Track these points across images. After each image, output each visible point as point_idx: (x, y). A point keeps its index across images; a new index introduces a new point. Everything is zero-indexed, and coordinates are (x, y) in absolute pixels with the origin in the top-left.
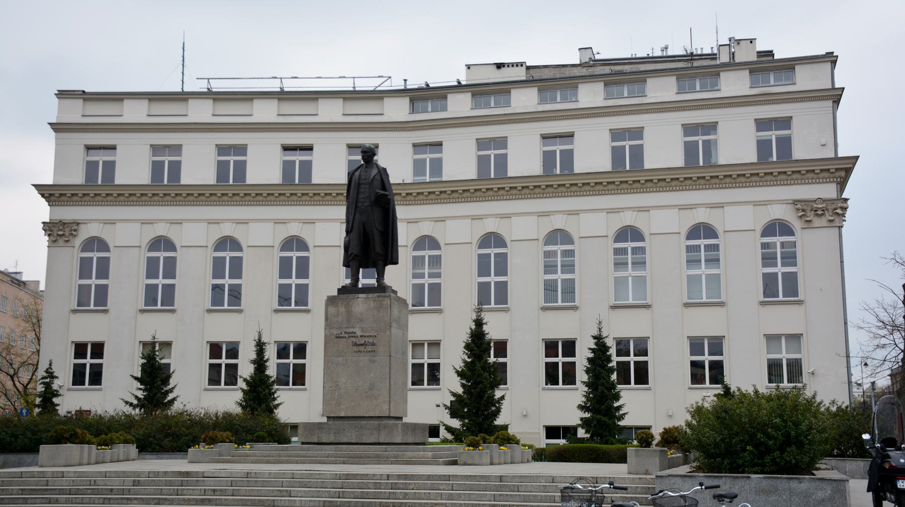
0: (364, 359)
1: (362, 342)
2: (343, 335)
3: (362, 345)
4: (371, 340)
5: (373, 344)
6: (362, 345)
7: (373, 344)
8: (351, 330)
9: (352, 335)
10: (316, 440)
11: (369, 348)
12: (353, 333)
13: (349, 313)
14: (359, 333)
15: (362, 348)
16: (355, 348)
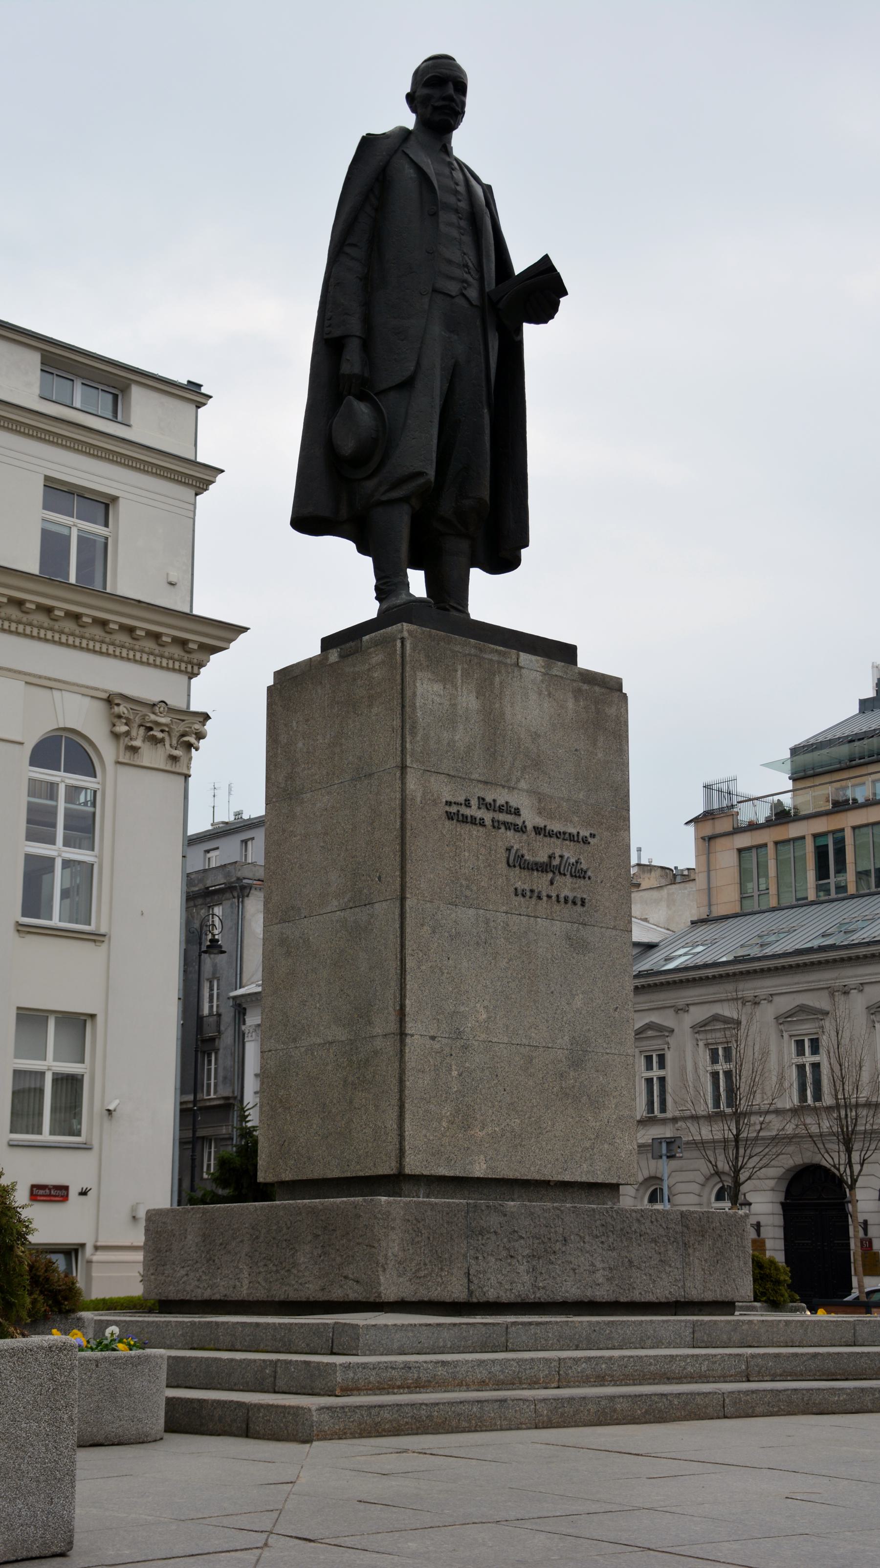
0: (550, 929)
1: (542, 858)
2: (473, 811)
3: (543, 868)
4: (569, 853)
5: (580, 874)
6: (543, 868)
7: (580, 874)
8: (502, 797)
9: (506, 818)
10: (457, 1291)
11: (566, 887)
12: (506, 808)
13: (493, 720)
14: (530, 817)
15: (540, 882)
16: (521, 880)
